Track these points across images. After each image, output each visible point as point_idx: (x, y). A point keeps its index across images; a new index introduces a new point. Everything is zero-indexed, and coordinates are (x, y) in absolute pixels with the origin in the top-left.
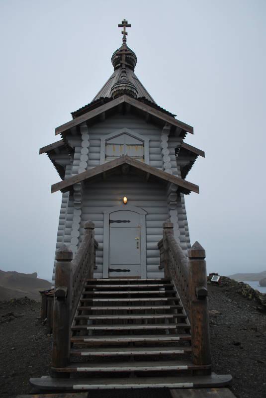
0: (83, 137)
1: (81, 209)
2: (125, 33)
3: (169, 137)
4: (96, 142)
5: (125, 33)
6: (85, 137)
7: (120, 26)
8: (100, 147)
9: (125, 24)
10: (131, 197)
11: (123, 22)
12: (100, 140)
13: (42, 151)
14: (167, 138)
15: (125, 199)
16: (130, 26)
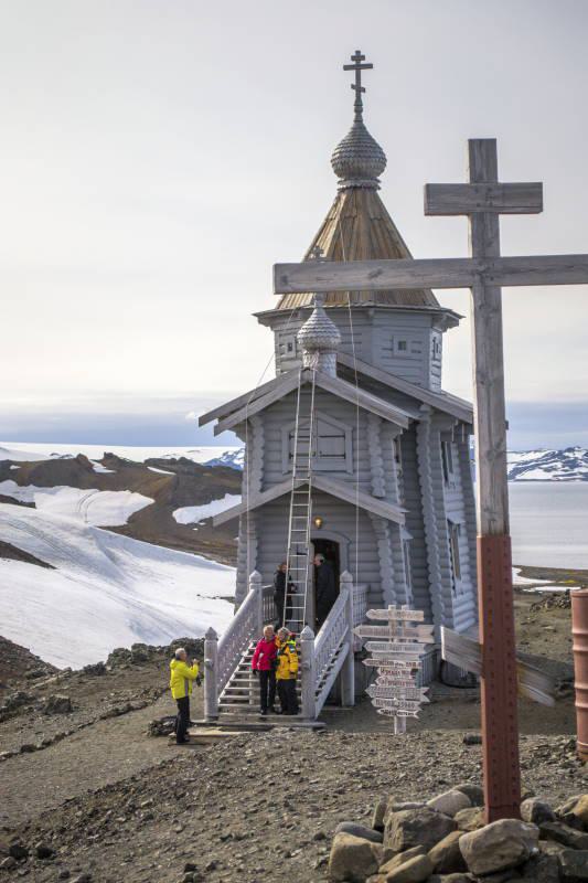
0: (255, 432)
1: (258, 538)
2: (358, 89)
3: (380, 426)
4: (275, 436)
5: (358, 89)
6: (259, 431)
7: (346, 68)
8: (280, 441)
9: (358, 64)
10: (325, 519)
11: (353, 58)
12: (280, 431)
13: (203, 420)
14: (378, 431)
15: (318, 522)
16: (370, 66)
